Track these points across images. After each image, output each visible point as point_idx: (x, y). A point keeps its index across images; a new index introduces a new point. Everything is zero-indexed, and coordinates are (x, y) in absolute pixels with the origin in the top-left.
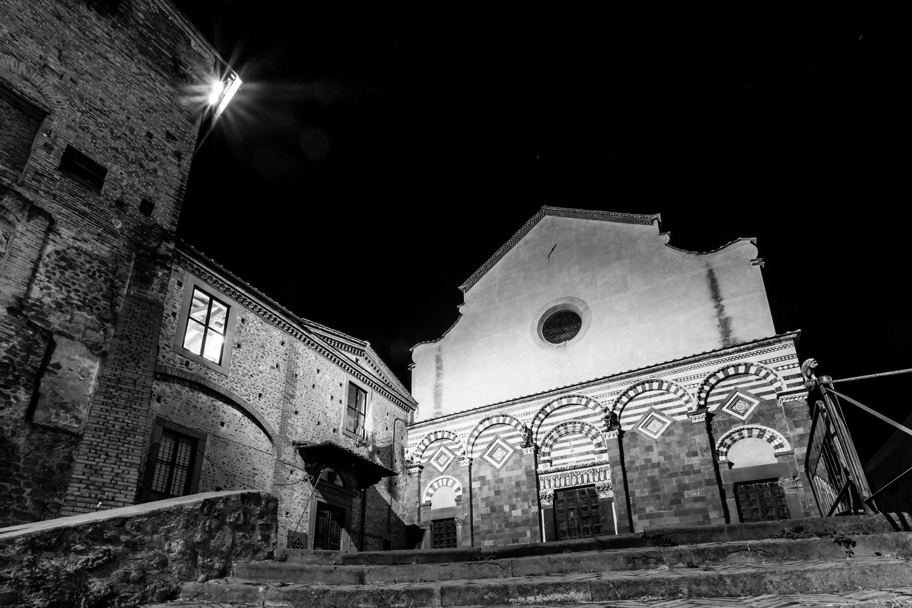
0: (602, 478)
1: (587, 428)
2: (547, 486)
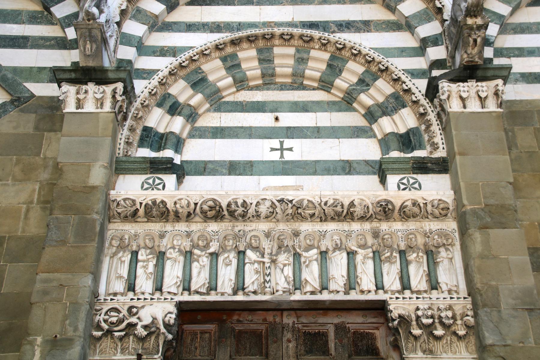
0: (417, 277)
1: (353, 71)
2: (145, 284)
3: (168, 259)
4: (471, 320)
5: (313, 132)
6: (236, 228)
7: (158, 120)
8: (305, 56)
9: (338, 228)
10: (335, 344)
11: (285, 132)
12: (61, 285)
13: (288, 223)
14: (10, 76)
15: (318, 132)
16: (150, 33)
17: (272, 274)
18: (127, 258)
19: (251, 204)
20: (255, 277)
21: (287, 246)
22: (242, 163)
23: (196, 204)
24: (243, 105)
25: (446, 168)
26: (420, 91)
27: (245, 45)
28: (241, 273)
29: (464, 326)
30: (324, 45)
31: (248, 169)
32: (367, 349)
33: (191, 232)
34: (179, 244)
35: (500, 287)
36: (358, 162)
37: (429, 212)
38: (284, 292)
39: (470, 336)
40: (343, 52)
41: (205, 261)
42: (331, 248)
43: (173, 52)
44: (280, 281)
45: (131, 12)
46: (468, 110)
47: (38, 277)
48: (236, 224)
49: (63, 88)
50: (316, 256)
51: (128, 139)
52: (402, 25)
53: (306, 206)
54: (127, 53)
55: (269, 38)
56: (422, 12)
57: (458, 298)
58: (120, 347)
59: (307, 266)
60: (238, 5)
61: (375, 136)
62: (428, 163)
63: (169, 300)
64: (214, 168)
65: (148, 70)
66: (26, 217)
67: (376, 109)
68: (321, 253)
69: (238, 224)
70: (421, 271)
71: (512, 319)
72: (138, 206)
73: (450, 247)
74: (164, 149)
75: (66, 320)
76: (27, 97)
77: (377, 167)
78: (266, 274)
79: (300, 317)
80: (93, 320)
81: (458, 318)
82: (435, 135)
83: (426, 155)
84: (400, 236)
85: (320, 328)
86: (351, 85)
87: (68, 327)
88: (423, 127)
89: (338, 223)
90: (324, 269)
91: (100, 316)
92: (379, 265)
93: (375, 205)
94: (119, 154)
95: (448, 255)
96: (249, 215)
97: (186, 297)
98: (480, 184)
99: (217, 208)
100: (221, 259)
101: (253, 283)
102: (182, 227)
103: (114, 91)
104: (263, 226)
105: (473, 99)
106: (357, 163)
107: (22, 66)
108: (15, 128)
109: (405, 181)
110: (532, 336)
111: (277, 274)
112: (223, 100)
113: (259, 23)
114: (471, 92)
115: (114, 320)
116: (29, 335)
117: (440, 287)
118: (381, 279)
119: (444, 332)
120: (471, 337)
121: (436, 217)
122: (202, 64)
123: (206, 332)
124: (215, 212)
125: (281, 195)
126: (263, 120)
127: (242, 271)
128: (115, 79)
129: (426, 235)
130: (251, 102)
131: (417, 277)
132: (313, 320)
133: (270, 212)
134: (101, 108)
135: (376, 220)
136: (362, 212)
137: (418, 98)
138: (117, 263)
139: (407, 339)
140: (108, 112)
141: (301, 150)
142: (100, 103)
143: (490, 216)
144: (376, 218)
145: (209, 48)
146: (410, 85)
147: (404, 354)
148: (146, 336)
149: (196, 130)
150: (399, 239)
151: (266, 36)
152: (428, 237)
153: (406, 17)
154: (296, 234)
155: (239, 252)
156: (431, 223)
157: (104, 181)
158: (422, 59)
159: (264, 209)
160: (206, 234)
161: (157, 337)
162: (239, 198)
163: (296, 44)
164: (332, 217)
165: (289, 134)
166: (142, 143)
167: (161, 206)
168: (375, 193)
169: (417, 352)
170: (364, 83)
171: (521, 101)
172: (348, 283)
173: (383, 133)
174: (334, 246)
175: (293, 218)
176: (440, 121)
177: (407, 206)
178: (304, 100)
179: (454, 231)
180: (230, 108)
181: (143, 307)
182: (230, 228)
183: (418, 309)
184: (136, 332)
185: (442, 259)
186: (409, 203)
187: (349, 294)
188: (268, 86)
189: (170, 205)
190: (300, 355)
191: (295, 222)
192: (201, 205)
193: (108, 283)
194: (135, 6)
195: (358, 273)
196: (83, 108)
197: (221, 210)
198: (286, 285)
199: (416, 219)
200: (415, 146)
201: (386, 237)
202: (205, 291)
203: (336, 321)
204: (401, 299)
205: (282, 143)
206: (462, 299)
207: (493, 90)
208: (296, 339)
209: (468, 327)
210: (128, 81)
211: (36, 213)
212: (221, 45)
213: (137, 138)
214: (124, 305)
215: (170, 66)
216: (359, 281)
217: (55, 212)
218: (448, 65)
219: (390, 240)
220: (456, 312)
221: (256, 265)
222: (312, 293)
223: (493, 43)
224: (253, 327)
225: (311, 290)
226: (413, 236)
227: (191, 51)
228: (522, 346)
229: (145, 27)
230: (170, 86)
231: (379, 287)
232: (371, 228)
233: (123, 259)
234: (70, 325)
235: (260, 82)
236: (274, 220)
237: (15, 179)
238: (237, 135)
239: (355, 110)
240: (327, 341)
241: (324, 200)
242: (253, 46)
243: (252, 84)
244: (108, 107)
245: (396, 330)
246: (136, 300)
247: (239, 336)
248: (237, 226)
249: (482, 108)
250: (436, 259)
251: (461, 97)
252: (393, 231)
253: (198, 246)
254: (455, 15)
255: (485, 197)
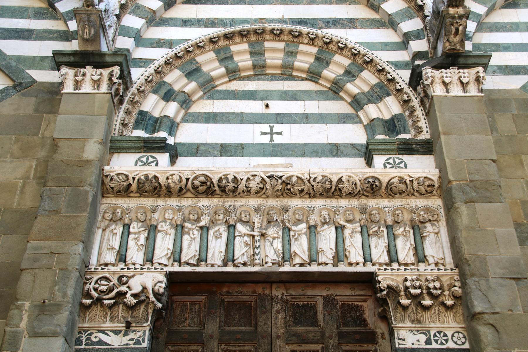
1: (339, 64)
2: (135, 255)
3: (159, 231)
4: (458, 290)
5: (302, 118)
6: (226, 203)
7: (152, 105)
8: (294, 49)
9: (326, 204)
10: (324, 315)
11: (275, 117)
12: (52, 252)
13: (277, 199)
14: (13, 63)
15: (306, 118)
16: (148, 27)
17: (262, 246)
18: (119, 230)
19: (242, 180)
20: (245, 249)
21: (277, 220)
22: (233, 145)
23: (187, 180)
24: (235, 94)
25: (430, 149)
26: (403, 81)
27: (237, 39)
28: (231, 246)
29: (452, 297)
30: (312, 40)
31: (239, 151)
32: (355, 321)
33: (183, 206)
34: (171, 218)
35: (487, 257)
36: (345, 145)
37: (416, 189)
38: (273, 264)
39: (457, 306)
40: (330, 46)
41: (196, 234)
42: (319, 223)
43: (170, 44)
44: (270, 254)
45: (130, 7)
46: (451, 94)
47: (29, 244)
48: (226, 199)
49: (62, 70)
50: (305, 230)
51: (124, 121)
52: (385, 22)
53: (295, 182)
54: (125, 43)
55: (260, 33)
56: (404, 11)
57: (445, 270)
58: (109, 315)
59: (296, 239)
60: (231, 4)
61: (361, 122)
62: (413, 144)
63: (159, 270)
64: (206, 150)
65: (145, 59)
66: (22, 192)
67: (362, 97)
68: (309, 228)
69: (228, 199)
70: (408, 245)
71: (500, 288)
72: (131, 181)
73: (435, 223)
74: (158, 131)
75: (55, 286)
76: (29, 83)
77: (363, 150)
78: (256, 247)
79: (289, 289)
80: (83, 289)
81: (446, 288)
82: (419, 119)
83: (410, 138)
84: (387, 212)
85: (309, 300)
86: (338, 76)
87: (56, 293)
88: (407, 113)
89: (326, 199)
90: (313, 243)
91: (90, 284)
92: (367, 239)
93: (362, 182)
94: (114, 134)
95: (434, 229)
96: (239, 191)
97: (176, 268)
98: (465, 161)
99: (209, 184)
100: (211, 232)
101: (243, 255)
102: (173, 202)
103: (111, 75)
104: (253, 202)
105: (455, 85)
106: (344, 146)
107: (26, 55)
108: (16, 110)
109: (391, 161)
110: (520, 304)
111: (266, 247)
112: (216, 89)
113: (251, 19)
114: (454, 78)
115: (104, 288)
116: (17, 300)
117: (427, 260)
118: (369, 252)
119: (432, 302)
120: (459, 308)
121: (421, 194)
122: (196, 56)
123: (196, 304)
124: (206, 188)
125: (271, 171)
126: (255, 107)
127: (232, 244)
128: (112, 62)
129: (412, 211)
130: (243, 91)
131: (405, 250)
132: (301, 293)
133: (260, 188)
134: (98, 90)
135: (363, 197)
136: (350, 189)
137: (402, 87)
138: (109, 236)
139: (396, 309)
140: (104, 93)
141: (290, 134)
142: (97, 83)
143: (475, 191)
144: (363, 195)
145: (203, 41)
146: (394, 75)
147: (392, 324)
148: (135, 304)
149: (189, 116)
150: (386, 215)
151: (258, 31)
152: (415, 213)
153: (390, 15)
154: (286, 210)
155: (229, 226)
156: (417, 200)
157: (98, 156)
158: (404, 52)
159: (254, 185)
160: (197, 209)
161: (147, 306)
162: (230, 174)
163: (286, 39)
164: (321, 193)
165: (278, 120)
166: (136, 126)
167: (154, 181)
168: (362, 171)
169: (406, 322)
170: (350, 74)
171: (499, 90)
172: (336, 256)
173: (369, 118)
174: (323, 221)
175: (282, 194)
176: (423, 107)
177: (394, 183)
178: (293, 89)
179: (439, 207)
180: (222, 96)
181: (133, 276)
182: (221, 203)
183: (406, 280)
184: (125, 300)
185: (428, 234)
186: (395, 180)
187: (337, 266)
188: (259, 77)
189: (162, 180)
190: (289, 326)
191: (285, 198)
192: (193, 180)
193: (99, 254)
194: (134, 3)
195: (346, 246)
196: (80, 89)
197: (212, 185)
198: (275, 258)
199: (403, 195)
200: (400, 130)
201: (374, 212)
202: (195, 262)
203: (325, 293)
204: (390, 270)
205: (272, 128)
206: (450, 271)
207: (474, 77)
208: (285, 310)
209: (455, 297)
210: (124, 65)
211: (32, 188)
212: (215, 38)
213: (133, 121)
214: (114, 274)
215: (165, 56)
216: (347, 254)
217: (49, 184)
218: (430, 56)
219: (377, 215)
220: (444, 283)
221: (246, 238)
222: (302, 265)
223: (471, 38)
224: (243, 298)
225: (300, 262)
226: (400, 212)
227: (186, 43)
228: (511, 314)
229: (144, 21)
230: (166, 74)
231: (367, 259)
232: (359, 205)
233: (115, 231)
234: (59, 291)
235: (252, 73)
236: (264, 196)
237: (13, 157)
238: (229, 120)
239: (342, 99)
240: (316, 313)
241: (313, 176)
242: (245, 40)
243: (243, 74)
244: (104, 88)
245: (386, 299)
246: (126, 270)
247: (229, 308)
248: (228, 202)
249: (464, 92)
250: (422, 234)
251: (444, 82)
252: (380, 207)
253: (189, 220)
254: (437, 7)
255: (470, 174)
